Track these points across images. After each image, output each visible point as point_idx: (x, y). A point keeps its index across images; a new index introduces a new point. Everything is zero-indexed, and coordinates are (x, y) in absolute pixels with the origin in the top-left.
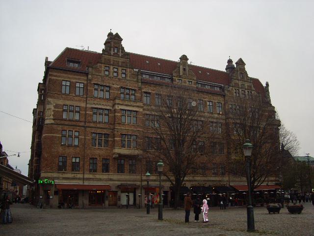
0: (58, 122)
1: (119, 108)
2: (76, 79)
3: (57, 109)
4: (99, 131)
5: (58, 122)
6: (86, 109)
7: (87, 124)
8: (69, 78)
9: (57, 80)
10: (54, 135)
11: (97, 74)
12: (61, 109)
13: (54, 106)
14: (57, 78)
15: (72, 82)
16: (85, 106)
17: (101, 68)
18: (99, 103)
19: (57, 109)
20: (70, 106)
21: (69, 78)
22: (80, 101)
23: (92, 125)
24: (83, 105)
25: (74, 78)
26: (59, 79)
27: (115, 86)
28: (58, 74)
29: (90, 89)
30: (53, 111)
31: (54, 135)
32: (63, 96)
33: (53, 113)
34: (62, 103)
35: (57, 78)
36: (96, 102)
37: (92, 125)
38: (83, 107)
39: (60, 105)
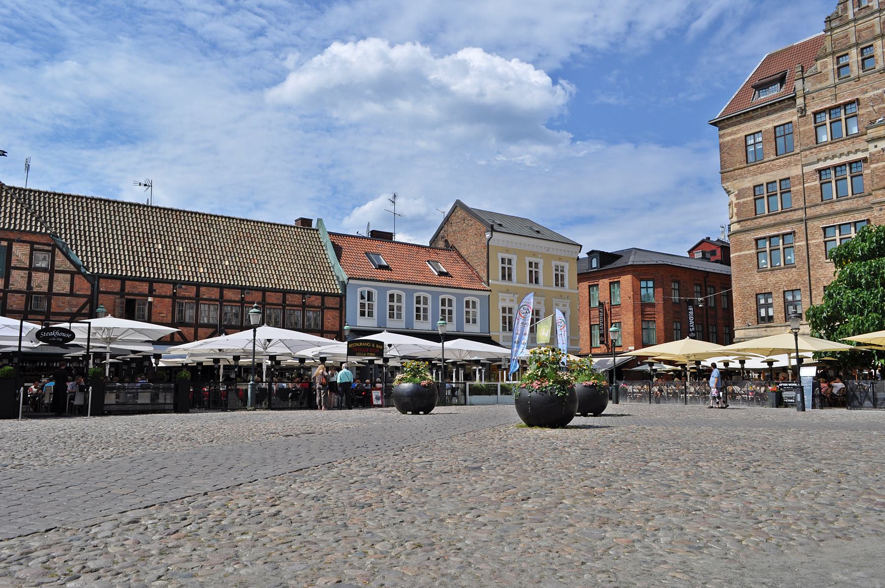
0: (749, 224)
1: (879, 149)
2: (773, 120)
3: (741, 201)
4: (838, 221)
5: (749, 224)
6: (803, 178)
7: (811, 212)
8: (758, 125)
9: (734, 140)
10: (742, 253)
11: (819, 86)
12: (749, 196)
13: (736, 195)
14: (733, 137)
15: (766, 131)
16: (801, 173)
17: (826, 67)
18: (830, 154)
19: (741, 201)
20: (767, 184)
21: (758, 125)
22: (787, 165)
23: (823, 209)
24: (795, 171)
25: (768, 123)
26: (739, 136)
27: (871, 94)
28: (735, 128)
29: (804, 131)
30: (736, 204)
31: (742, 253)
32: (751, 168)
33: (735, 210)
34: (751, 185)
35: (733, 137)
36: (822, 155)
37: (823, 209)
38: (797, 176)
39: (749, 188)
